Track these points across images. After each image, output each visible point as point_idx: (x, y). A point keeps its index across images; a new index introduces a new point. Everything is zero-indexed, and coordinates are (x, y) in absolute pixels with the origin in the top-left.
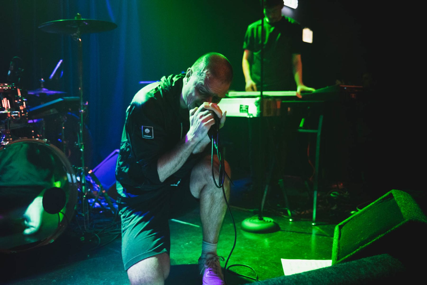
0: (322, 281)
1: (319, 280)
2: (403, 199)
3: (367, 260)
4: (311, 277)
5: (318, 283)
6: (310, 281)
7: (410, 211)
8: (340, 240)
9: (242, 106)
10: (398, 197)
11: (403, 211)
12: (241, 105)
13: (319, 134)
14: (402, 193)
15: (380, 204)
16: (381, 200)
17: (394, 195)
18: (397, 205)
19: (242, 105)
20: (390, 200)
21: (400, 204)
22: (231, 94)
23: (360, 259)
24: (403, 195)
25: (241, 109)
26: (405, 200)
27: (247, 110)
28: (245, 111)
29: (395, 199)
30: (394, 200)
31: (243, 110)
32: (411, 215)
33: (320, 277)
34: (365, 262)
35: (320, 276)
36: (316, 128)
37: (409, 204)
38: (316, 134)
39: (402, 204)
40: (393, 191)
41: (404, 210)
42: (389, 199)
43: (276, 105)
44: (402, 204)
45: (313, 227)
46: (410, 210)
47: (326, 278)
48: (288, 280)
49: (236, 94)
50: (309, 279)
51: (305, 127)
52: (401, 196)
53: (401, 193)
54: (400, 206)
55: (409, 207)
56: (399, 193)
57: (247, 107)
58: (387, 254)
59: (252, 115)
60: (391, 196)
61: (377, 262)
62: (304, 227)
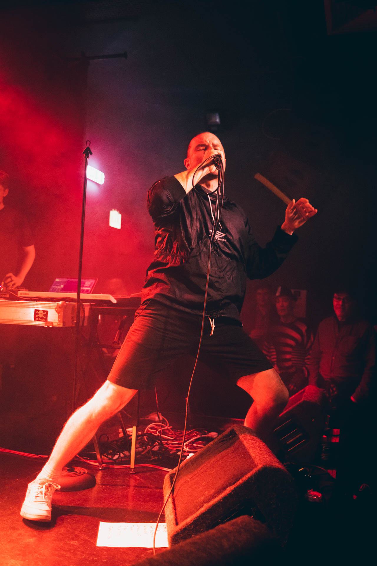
9: (37, 312)
12: (36, 310)
19: (39, 310)
22: (21, 294)
25: (37, 316)
27: (45, 317)
28: (42, 318)
31: (39, 317)
49: (28, 294)
57: (45, 313)
59: (52, 323)
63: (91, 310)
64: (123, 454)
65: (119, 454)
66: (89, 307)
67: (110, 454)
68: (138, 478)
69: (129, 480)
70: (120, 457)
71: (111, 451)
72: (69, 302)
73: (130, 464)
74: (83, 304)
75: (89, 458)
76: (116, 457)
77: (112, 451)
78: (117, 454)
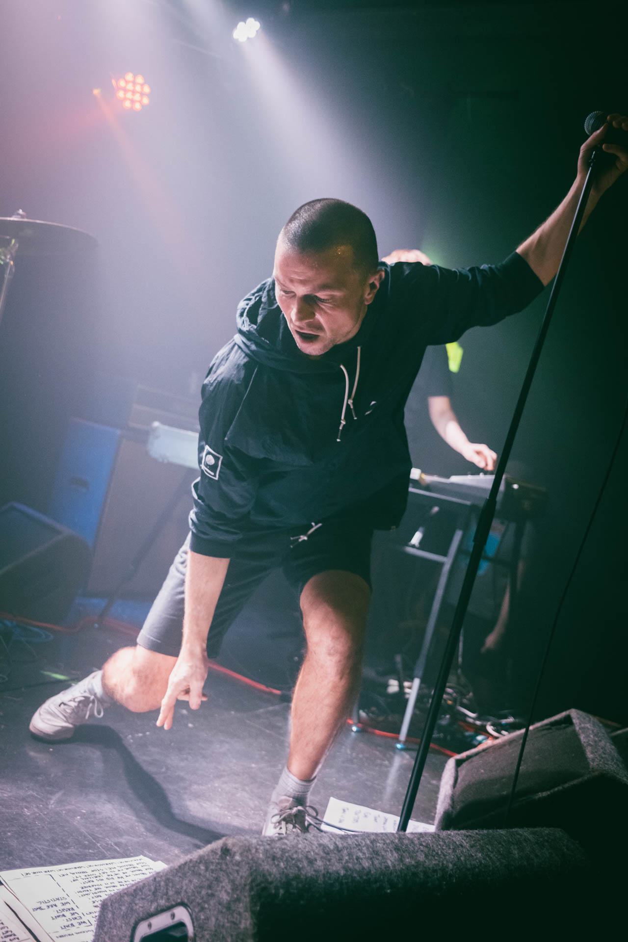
0: (442, 856)
1: (437, 853)
2: (591, 732)
3: (525, 833)
4: (424, 844)
5: (436, 858)
6: (422, 851)
7: (602, 758)
8: (456, 789)
10: (583, 725)
11: (590, 756)
13: (446, 568)
14: (590, 719)
15: (545, 732)
16: (547, 725)
17: (575, 721)
18: (579, 740)
20: (565, 728)
21: (584, 740)
23: (512, 828)
24: (592, 725)
26: (595, 735)
29: (577, 728)
30: (574, 731)
32: (605, 767)
33: (439, 847)
34: (521, 835)
35: (440, 845)
36: (445, 553)
37: (602, 743)
38: (440, 565)
39: (589, 741)
40: (574, 713)
41: (592, 753)
42: (563, 725)
44: (589, 741)
45: (397, 751)
46: (603, 756)
47: (450, 851)
48: (383, 842)
50: (421, 847)
51: (423, 545)
52: (588, 725)
53: (587, 719)
54: (585, 745)
55: (602, 748)
56: (584, 719)
58: (560, 829)
60: (568, 720)
61: (541, 839)
62: (379, 748)
67: (373, 713)
71: (373, 709)
76: (381, 718)
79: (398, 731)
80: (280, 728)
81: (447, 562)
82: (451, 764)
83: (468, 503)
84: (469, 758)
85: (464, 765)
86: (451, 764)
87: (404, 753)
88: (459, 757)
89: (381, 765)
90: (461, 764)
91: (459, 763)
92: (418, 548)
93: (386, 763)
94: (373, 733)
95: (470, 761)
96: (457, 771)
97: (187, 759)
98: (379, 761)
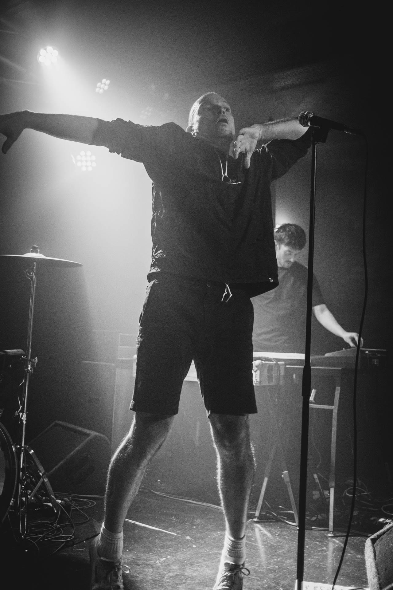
38: (331, 411)
43: (279, 370)
63: (286, 368)
64: (321, 516)
65: (316, 516)
66: (284, 366)
68: (337, 542)
69: (328, 543)
70: (318, 519)
72: (264, 361)
73: (328, 527)
74: (278, 364)
75: (286, 518)
76: (314, 518)
77: (309, 513)
78: (315, 516)
79: (327, 525)
80: (251, 537)
81: (335, 408)
82: (368, 542)
83: (341, 369)
84: (379, 536)
85: (378, 542)
86: (368, 542)
87: (334, 539)
88: (372, 537)
89: (322, 550)
90: (376, 542)
91: (374, 541)
92: (314, 403)
93: (325, 548)
94: (312, 529)
95: (381, 538)
96: (374, 547)
97: (197, 570)
98: (320, 549)
